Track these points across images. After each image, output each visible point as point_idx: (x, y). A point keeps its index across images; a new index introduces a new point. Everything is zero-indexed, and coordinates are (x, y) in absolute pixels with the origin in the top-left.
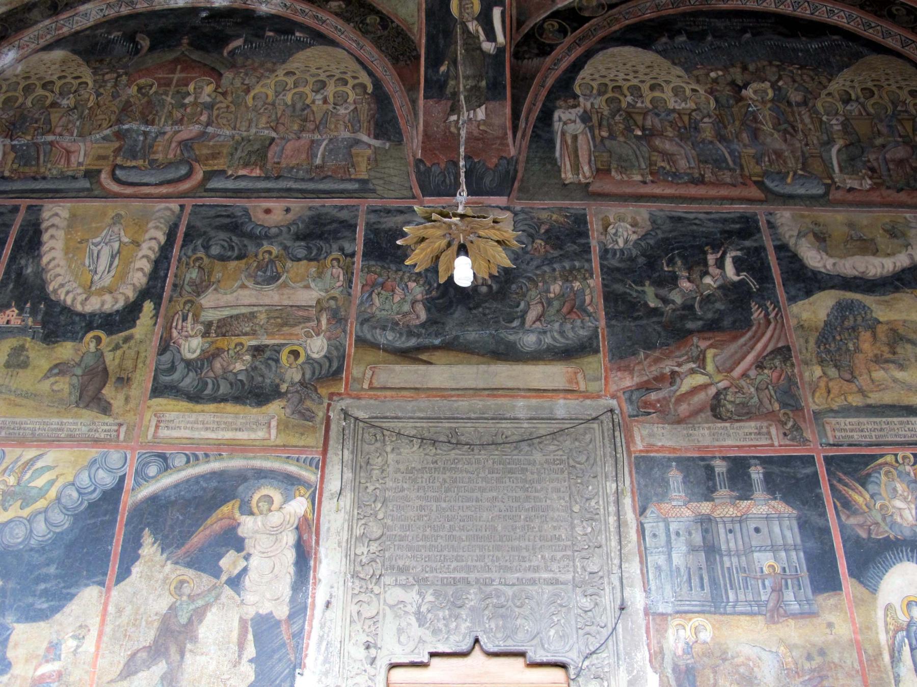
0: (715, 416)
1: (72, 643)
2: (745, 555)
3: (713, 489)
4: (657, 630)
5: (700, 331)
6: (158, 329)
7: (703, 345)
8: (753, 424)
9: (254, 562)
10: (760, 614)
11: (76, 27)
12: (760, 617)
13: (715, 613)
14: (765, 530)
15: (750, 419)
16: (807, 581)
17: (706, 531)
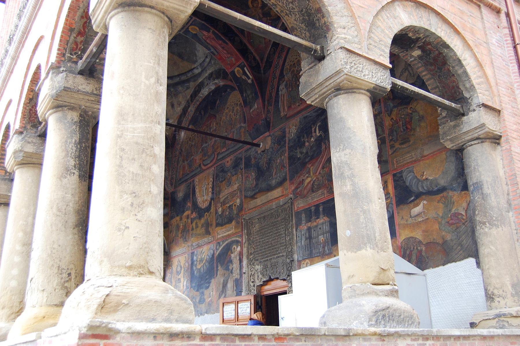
0: (312, 192)
1: (212, 293)
2: (317, 237)
3: (311, 218)
4: (299, 266)
5: (309, 161)
6: (215, 208)
7: (309, 166)
8: (320, 191)
9: (234, 266)
10: (320, 256)
11: (192, 115)
12: (320, 257)
13: (310, 258)
14: (322, 228)
15: (320, 189)
16: (330, 243)
17: (309, 232)
